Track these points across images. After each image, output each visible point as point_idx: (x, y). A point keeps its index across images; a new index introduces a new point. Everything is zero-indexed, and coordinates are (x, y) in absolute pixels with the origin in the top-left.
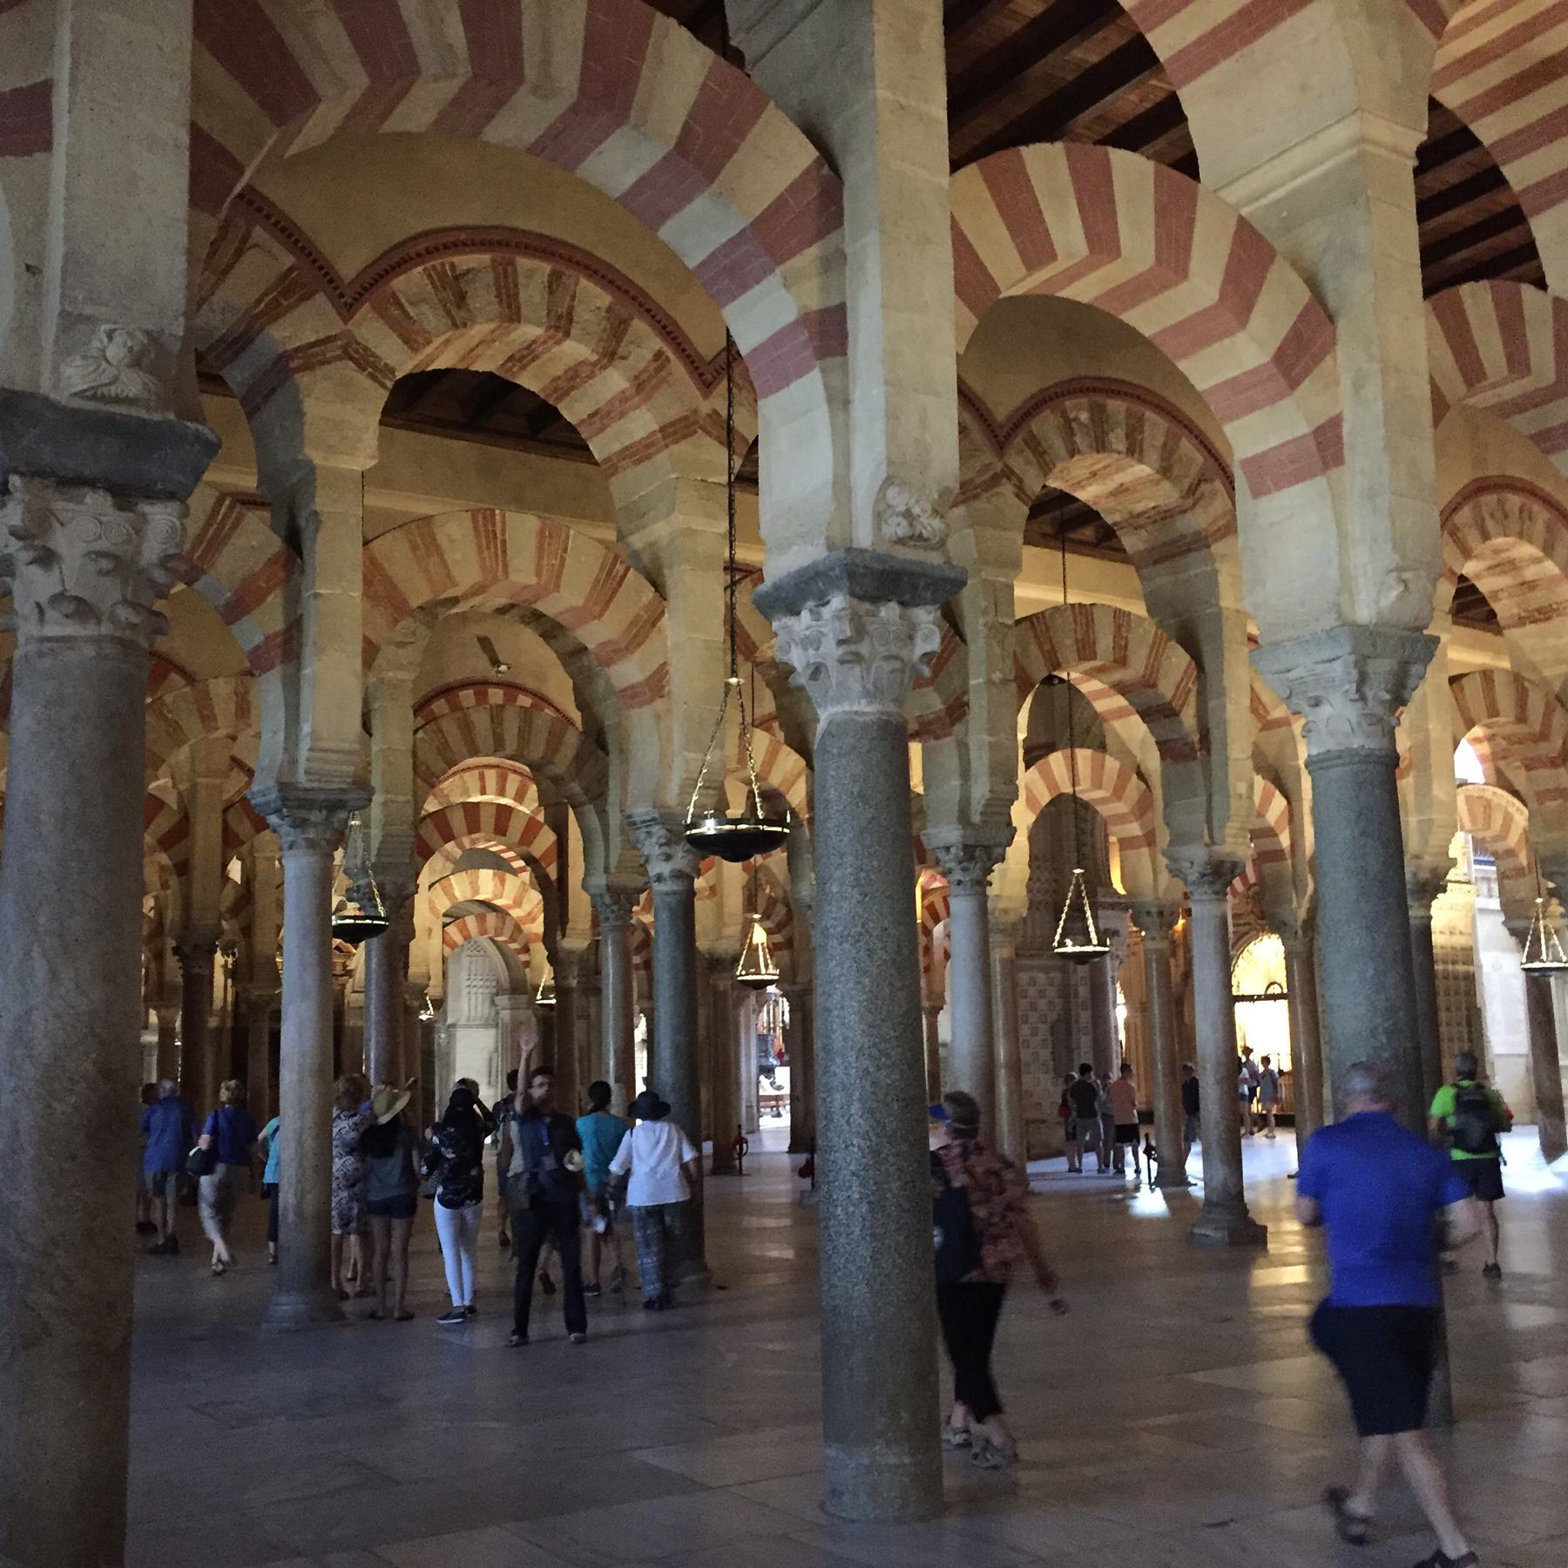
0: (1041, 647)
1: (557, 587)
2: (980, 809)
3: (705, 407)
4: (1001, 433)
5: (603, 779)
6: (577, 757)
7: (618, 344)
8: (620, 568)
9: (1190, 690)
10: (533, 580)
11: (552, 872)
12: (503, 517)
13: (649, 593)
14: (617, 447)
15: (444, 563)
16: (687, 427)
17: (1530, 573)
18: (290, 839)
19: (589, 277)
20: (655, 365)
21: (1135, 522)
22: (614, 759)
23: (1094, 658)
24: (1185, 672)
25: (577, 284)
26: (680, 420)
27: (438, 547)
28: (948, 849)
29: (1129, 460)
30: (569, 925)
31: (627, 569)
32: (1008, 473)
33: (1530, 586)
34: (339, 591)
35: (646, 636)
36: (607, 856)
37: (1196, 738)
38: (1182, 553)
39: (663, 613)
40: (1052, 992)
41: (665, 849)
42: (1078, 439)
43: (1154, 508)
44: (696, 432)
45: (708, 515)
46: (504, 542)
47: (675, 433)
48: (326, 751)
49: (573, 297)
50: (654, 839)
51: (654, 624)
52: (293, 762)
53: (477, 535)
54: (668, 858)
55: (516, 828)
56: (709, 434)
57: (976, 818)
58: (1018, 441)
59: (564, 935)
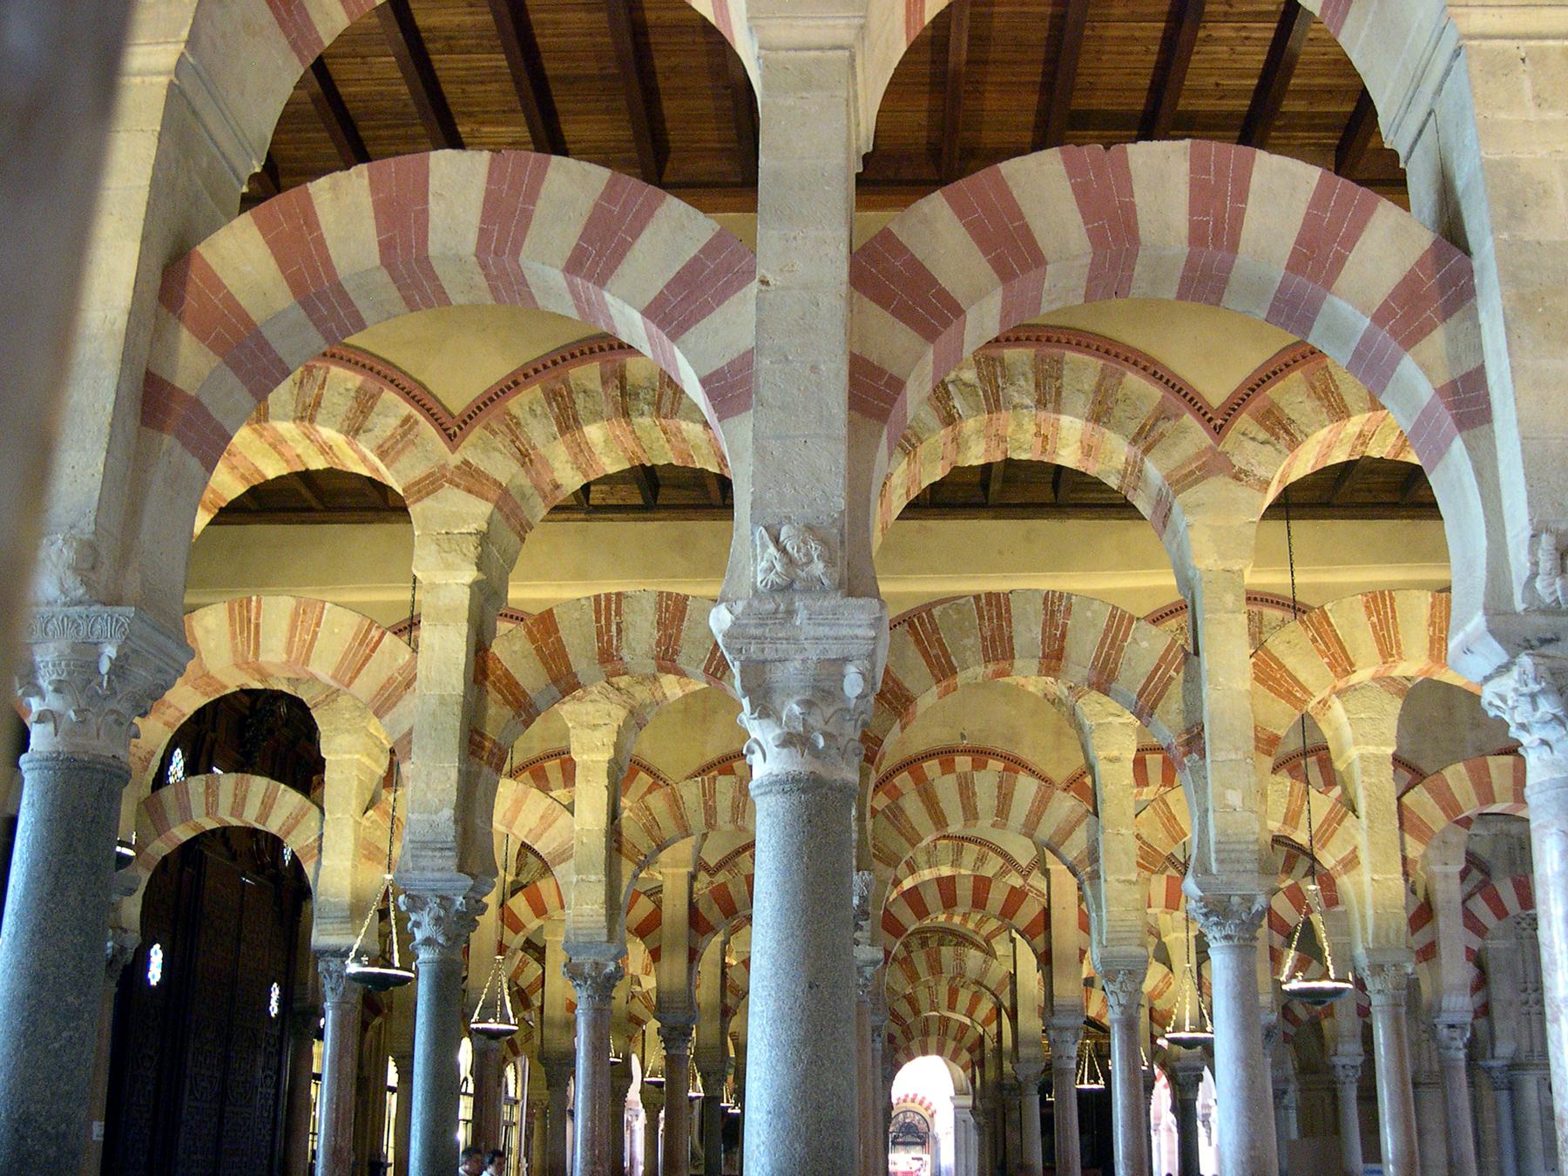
3: (454, 459)
7: (366, 418)
8: (375, 633)
12: (259, 602)
16: (433, 483)
19: (337, 364)
20: (400, 431)
24: (1163, 658)
25: (327, 373)
26: (427, 477)
31: (383, 634)
35: (400, 697)
42: (958, 403)
44: (442, 486)
45: (449, 567)
46: (257, 626)
47: (419, 491)
49: (322, 387)
51: (408, 686)
53: (232, 624)
56: (458, 486)
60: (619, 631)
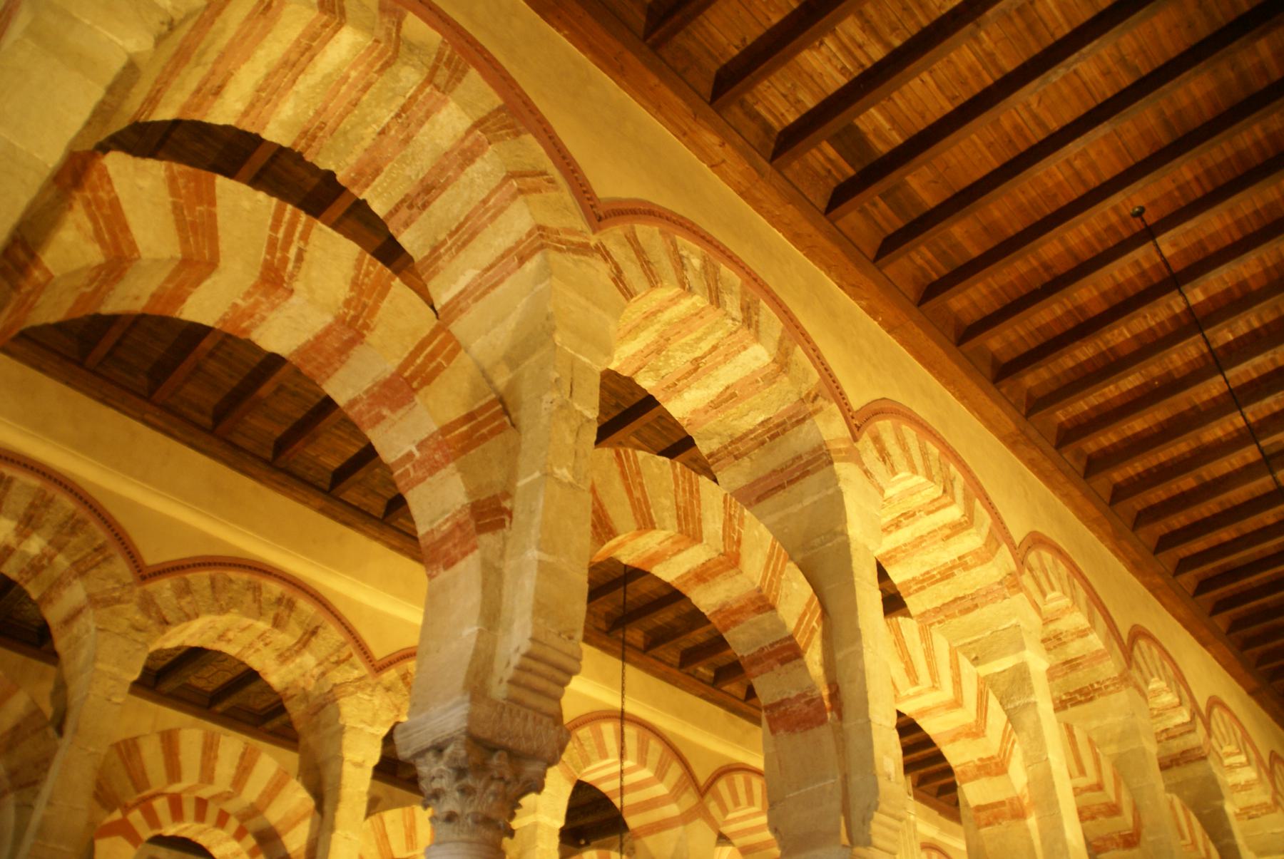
0: (629, 492)
2: (510, 673)
9: (813, 631)
17: (1075, 648)
33: (1071, 664)
37: (825, 693)
43: (762, 423)
57: (499, 691)
60: (300, 258)
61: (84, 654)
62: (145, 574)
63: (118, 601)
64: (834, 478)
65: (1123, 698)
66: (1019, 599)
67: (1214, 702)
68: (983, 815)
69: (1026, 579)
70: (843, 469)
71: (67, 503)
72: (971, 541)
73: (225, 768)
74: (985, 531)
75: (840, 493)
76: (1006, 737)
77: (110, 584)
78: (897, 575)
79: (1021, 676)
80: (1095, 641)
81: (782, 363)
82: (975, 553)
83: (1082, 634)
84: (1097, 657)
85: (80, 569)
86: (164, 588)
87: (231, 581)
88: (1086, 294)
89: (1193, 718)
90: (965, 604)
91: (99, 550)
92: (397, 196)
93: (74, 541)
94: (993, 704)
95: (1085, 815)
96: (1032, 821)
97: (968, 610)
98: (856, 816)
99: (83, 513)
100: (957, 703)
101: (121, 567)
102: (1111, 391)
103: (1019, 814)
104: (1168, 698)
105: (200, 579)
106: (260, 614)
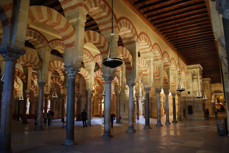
1: (59, 24)
2: (112, 72)
4: (118, 21)
5: (42, 66)
6: (38, 63)
10: (56, 22)
11: (25, 81)
13: (73, 29)
14: (68, 6)
15: (42, 14)
17: (157, 55)
18: (8, 59)
21: (125, 39)
22: (44, 64)
23: (123, 54)
27: (41, 11)
28: (106, 77)
29: (129, 30)
30: (27, 89)
32: (117, 26)
33: (156, 56)
34: (24, 12)
36: (42, 77)
37: (132, 67)
38: (131, 43)
39: (74, 33)
40: (85, 101)
41: (72, 71)
44: (82, 6)
46: (52, 14)
48: (18, 41)
50: (70, 70)
52: (11, 43)
54: (72, 73)
55: (21, 75)
56: (84, 7)
57: (111, 73)
58: (119, 22)
59: (26, 90)
61: (42, 53)
62: (48, 42)
63: (46, 46)
64: (135, 44)
65: (161, 61)
66: (152, 53)
67: (173, 58)
68: (144, 75)
69: (153, 50)
70: (136, 43)
71: (38, 34)
72: (148, 46)
73: (59, 65)
74: (149, 45)
75: (136, 46)
76: (147, 68)
77: (45, 44)
78: (140, 52)
79: (150, 61)
80: (159, 55)
81: (132, 32)
82: (148, 48)
83: (158, 54)
84: (159, 56)
85: (41, 43)
86: (50, 44)
87: (57, 42)
88: (167, 19)
89: (169, 62)
90: (146, 52)
91: (43, 40)
92: (97, 18)
93: (40, 39)
94: (147, 64)
95: (154, 76)
96: (149, 76)
97: (146, 53)
98: (134, 78)
99: (40, 35)
100: (143, 65)
101: (45, 42)
102: (168, 27)
103: (147, 75)
104: (167, 59)
105: (54, 42)
106: (61, 46)
